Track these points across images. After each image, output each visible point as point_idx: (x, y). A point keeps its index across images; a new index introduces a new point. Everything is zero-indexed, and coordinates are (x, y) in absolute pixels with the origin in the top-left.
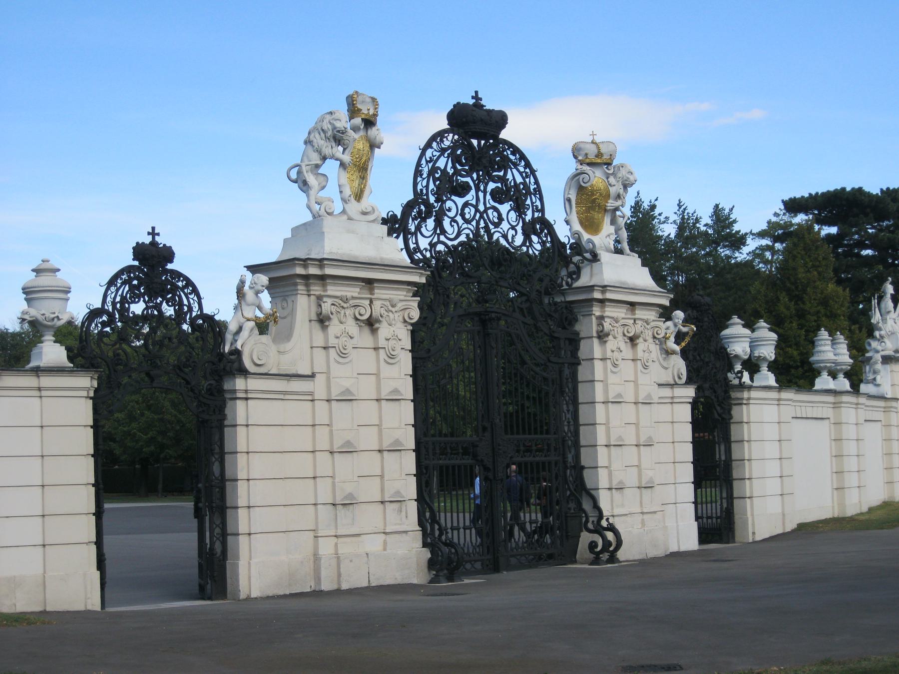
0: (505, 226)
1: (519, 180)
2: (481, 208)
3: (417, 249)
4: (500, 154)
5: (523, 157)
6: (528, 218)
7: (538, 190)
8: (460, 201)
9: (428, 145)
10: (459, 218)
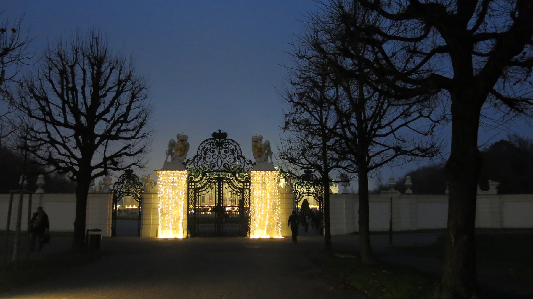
0: (227, 158)
1: (233, 147)
2: (219, 155)
3: (197, 166)
4: (228, 142)
5: (235, 142)
6: (236, 156)
7: (240, 149)
8: (212, 154)
9: (202, 143)
10: (211, 158)
